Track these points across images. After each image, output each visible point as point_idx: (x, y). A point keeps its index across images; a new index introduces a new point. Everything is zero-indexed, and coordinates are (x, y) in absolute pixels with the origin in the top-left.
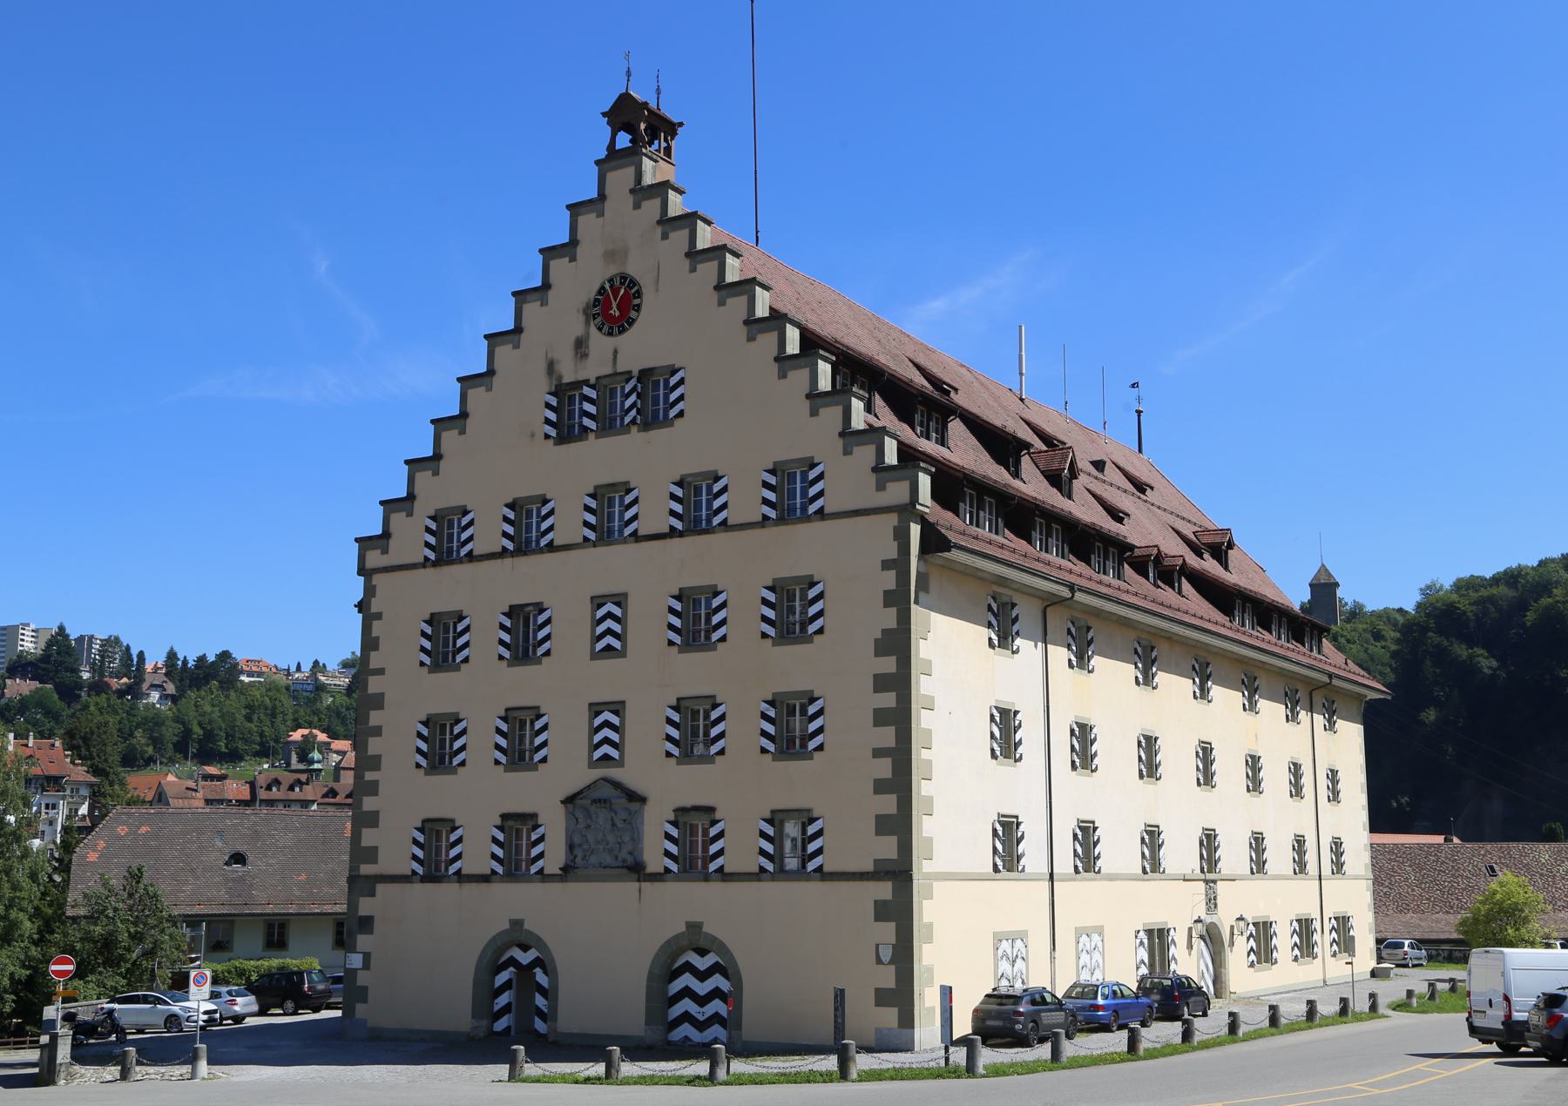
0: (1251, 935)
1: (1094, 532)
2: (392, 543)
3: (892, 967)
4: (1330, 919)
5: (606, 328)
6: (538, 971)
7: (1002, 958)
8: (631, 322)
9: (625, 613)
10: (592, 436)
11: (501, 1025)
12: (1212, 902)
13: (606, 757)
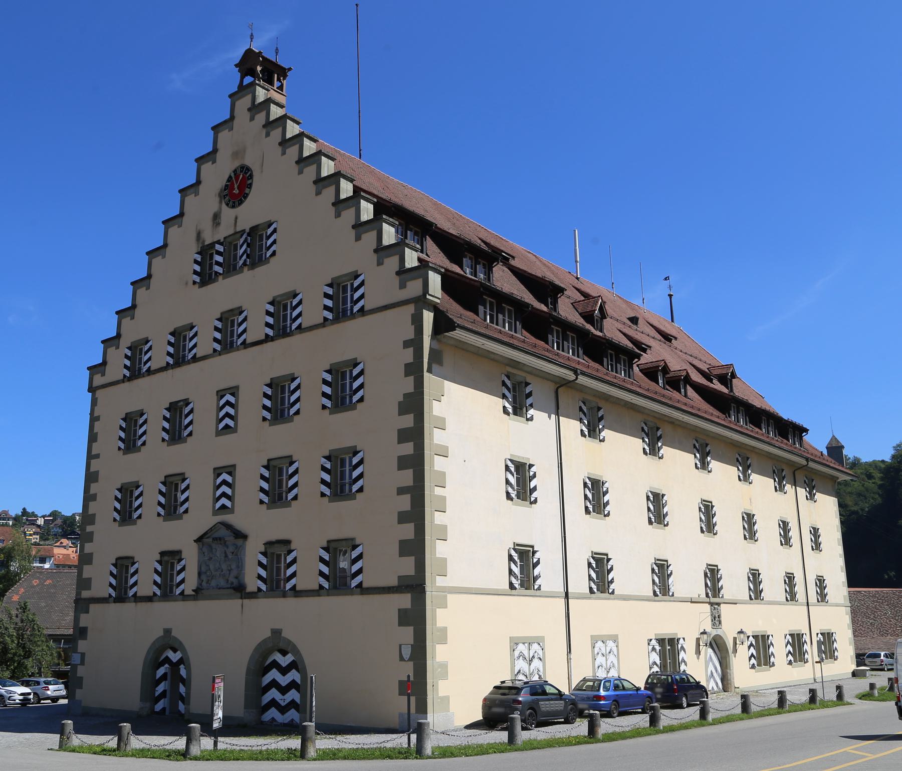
0: (751, 645)
1: (604, 341)
2: (108, 368)
3: (411, 664)
4: (817, 634)
5: (231, 203)
6: (182, 667)
7: (519, 658)
8: (246, 196)
9: (237, 401)
10: (220, 278)
11: (159, 707)
12: (716, 620)
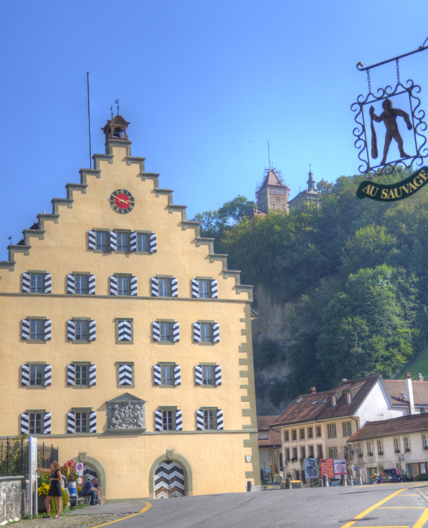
13: (125, 384)
